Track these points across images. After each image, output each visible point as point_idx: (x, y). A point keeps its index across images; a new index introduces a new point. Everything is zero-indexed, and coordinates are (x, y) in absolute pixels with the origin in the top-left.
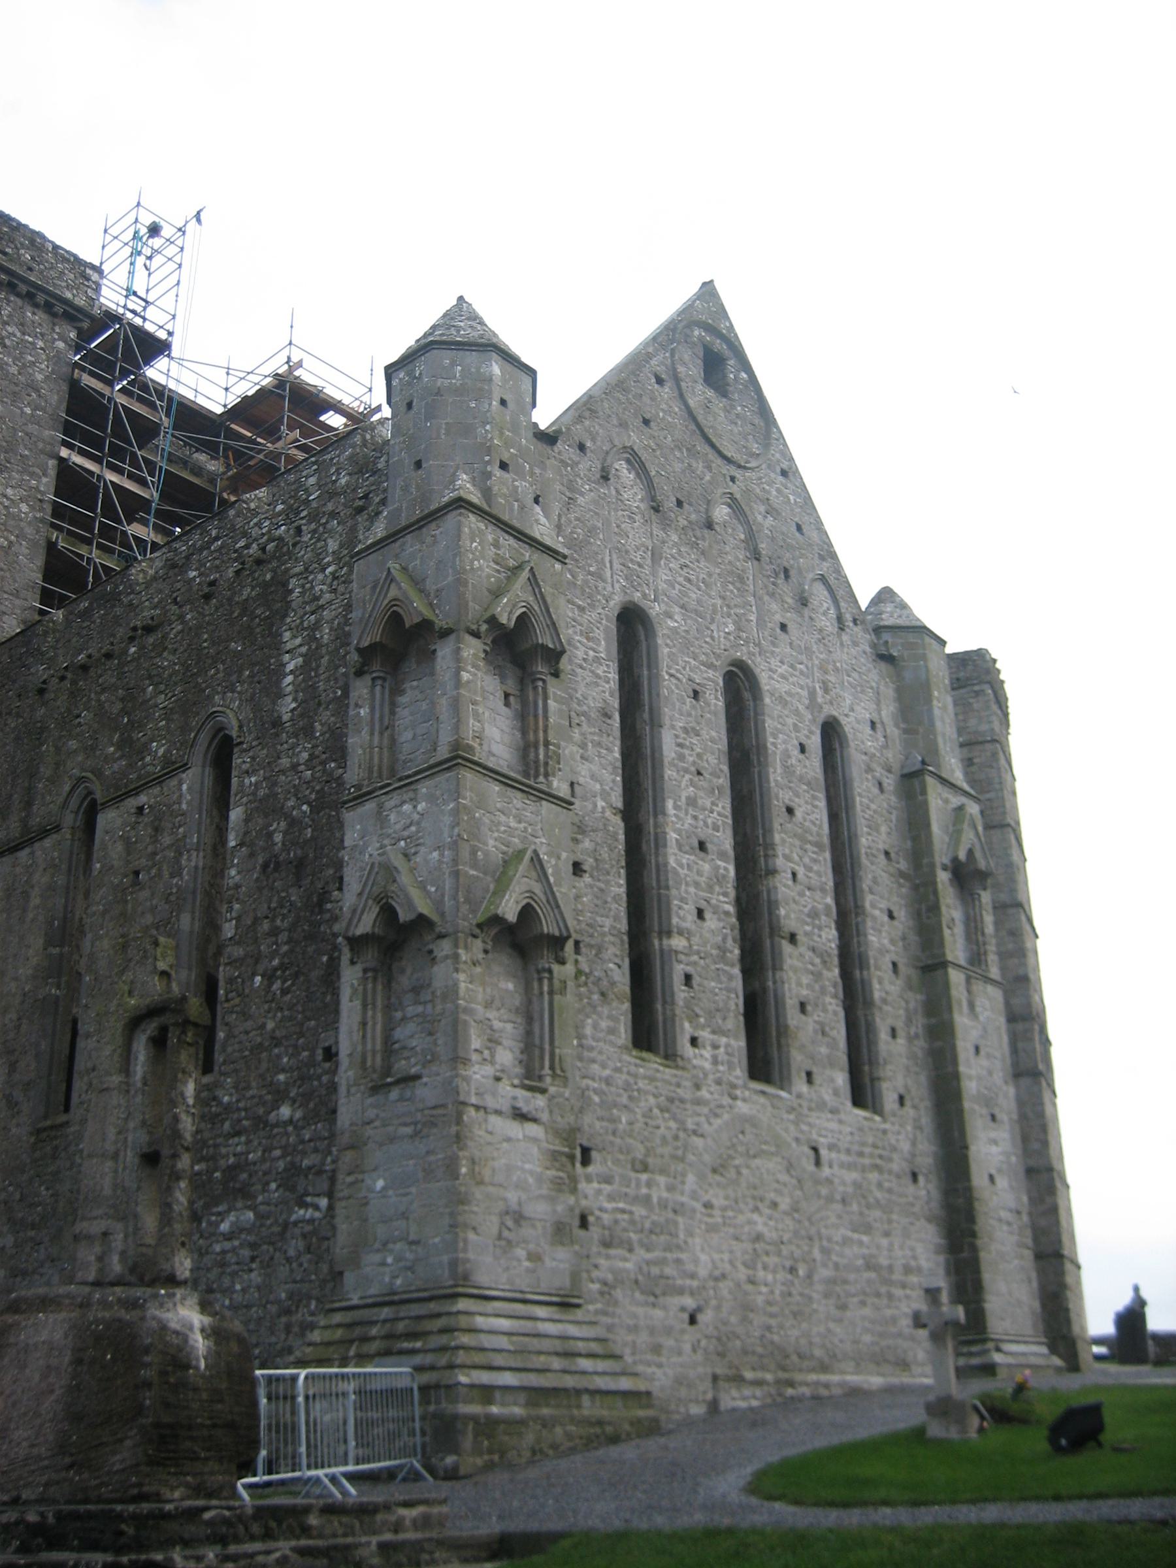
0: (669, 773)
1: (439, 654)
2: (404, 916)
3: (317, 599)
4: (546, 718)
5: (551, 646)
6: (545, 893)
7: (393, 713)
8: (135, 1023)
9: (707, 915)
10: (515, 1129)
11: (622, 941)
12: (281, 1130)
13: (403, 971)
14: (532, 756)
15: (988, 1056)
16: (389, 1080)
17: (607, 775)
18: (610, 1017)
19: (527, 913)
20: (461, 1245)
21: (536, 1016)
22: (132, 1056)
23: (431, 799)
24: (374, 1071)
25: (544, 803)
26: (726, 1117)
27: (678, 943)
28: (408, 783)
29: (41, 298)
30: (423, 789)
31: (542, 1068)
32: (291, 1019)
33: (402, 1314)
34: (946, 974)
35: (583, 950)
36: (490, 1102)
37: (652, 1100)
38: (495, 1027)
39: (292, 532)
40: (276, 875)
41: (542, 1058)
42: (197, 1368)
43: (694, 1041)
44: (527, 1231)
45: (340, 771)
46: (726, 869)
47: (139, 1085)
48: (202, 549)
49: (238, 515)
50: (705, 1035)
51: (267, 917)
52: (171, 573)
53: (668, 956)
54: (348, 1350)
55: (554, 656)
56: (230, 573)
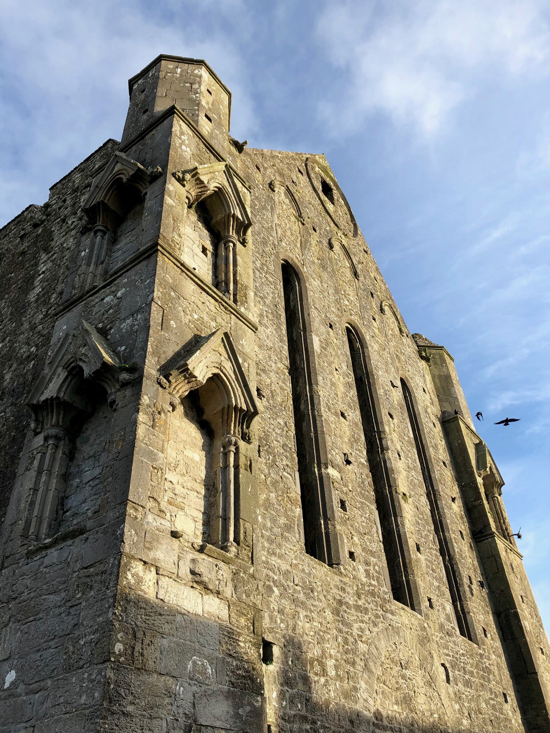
5: (240, 217)
11: (292, 458)
25: (232, 316)
38: (177, 492)
43: (351, 555)
46: (359, 435)
50: (358, 551)
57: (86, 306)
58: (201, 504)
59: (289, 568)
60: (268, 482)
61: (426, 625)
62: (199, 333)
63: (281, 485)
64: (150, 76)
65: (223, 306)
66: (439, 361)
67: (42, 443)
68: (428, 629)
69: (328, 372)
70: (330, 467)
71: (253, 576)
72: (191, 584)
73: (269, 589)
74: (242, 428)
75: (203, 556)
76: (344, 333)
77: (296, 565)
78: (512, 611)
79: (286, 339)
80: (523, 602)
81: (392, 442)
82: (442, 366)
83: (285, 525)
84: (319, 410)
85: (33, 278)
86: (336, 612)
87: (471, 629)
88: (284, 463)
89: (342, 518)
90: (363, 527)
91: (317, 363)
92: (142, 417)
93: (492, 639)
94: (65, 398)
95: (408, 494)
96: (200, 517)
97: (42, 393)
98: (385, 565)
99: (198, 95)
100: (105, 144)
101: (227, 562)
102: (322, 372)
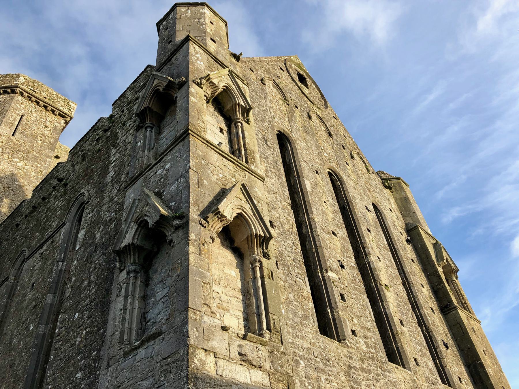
5: (243, 104)
25: (246, 172)
29: (49, 108)
38: (222, 299)
43: (353, 332)
46: (347, 246)
50: (358, 329)
57: (145, 179)
58: (240, 306)
59: (309, 346)
60: (287, 286)
61: (415, 378)
62: (224, 187)
63: (296, 288)
64: (170, 18)
65: (239, 166)
66: (398, 188)
67: (126, 276)
68: (417, 381)
69: (319, 204)
70: (329, 271)
71: (283, 353)
72: (240, 362)
73: (297, 362)
74: (263, 249)
75: (246, 342)
76: (327, 176)
77: (314, 343)
78: (478, 362)
79: (286, 184)
80: (485, 355)
81: (372, 249)
82: (401, 191)
83: (303, 315)
84: (317, 232)
85: (108, 166)
86: (348, 374)
87: (449, 379)
88: (296, 272)
89: (343, 306)
90: (359, 311)
91: (310, 199)
92: (192, 249)
93: (466, 384)
94: (138, 243)
95: (389, 285)
96: (241, 315)
97: (122, 242)
98: (379, 337)
99: (204, 26)
100: (146, 69)
101: (264, 344)
102: (315, 205)
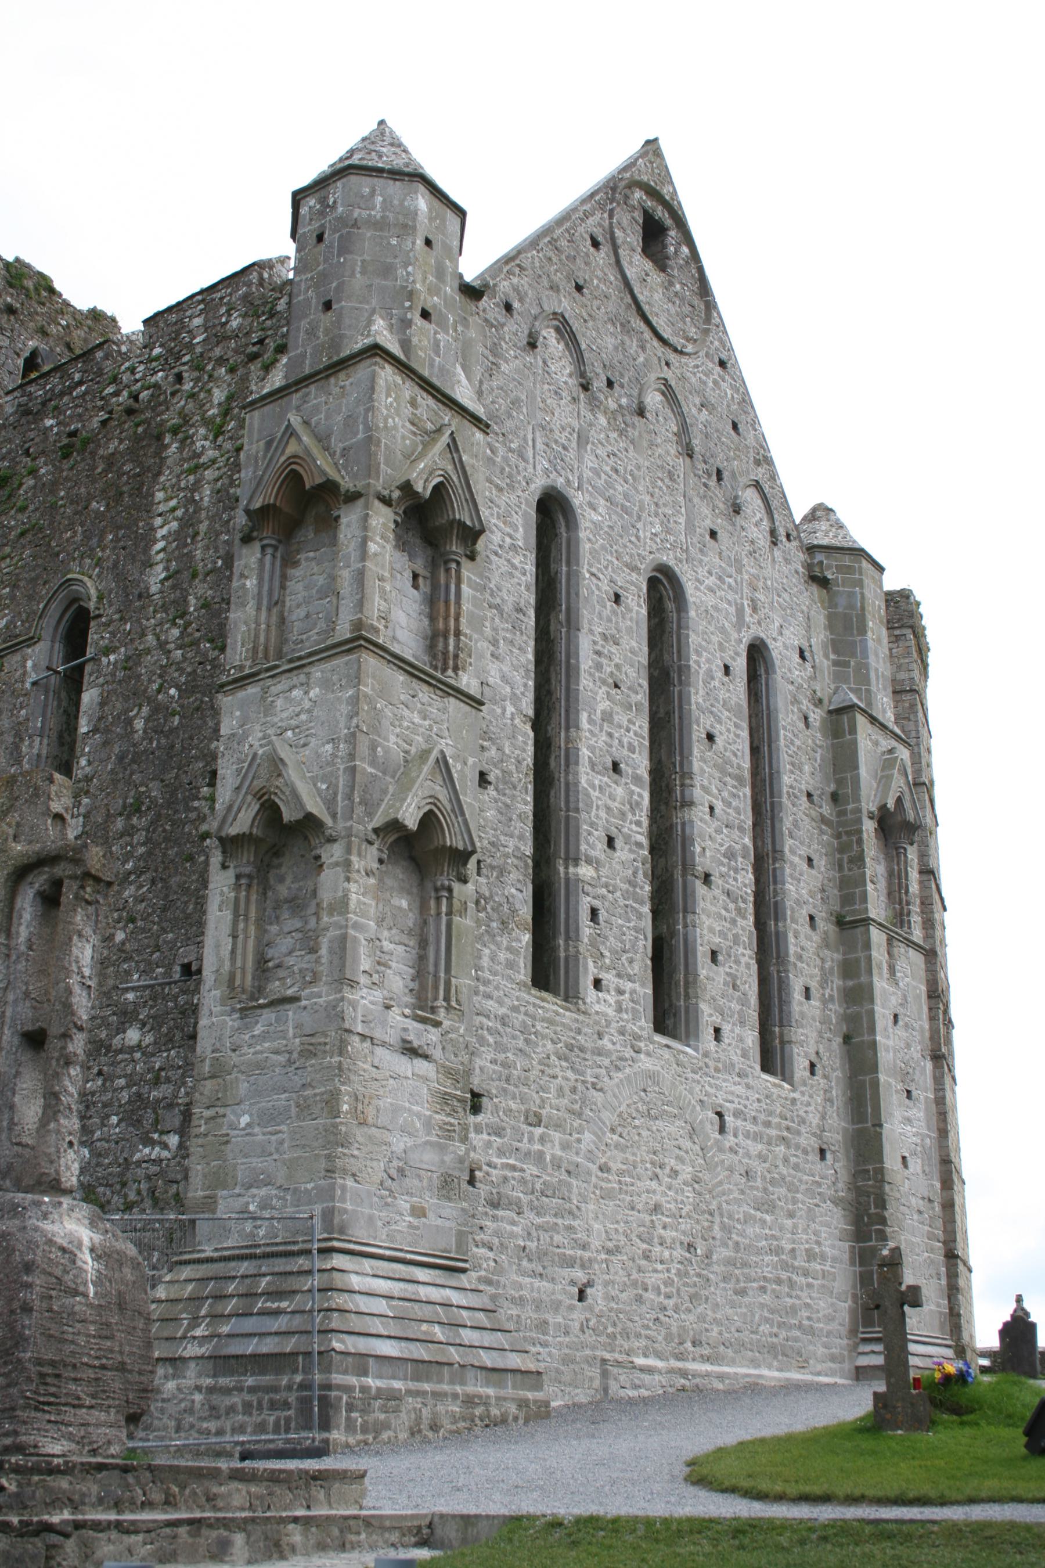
0: (586, 682)
1: (344, 521)
2: (288, 815)
3: (199, 456)
4: (458, 603)
5: (469, 523)
6: (450, 801)
7: (283, 587)
8: (22, 873)
9: (619, 843)
10: (405, 1065)
11: (526, 865)
12: (127, 1056)
13: (281, 880)
14: (440, 646)
15: (907, 1026)
16: (261, 1001)
17: (518, 678)
18: (509, 949)
19: (429, 820)
20: (339, 1192)
21: (432, 939)
22: (15, 914)
23: (326, 684)
24: (243, 991)
25: (452, 700)
26: (627, 1070)
27: (585, 871)
28: (299, 665)
30: (317, 672)
31: (436, 999)
32: (143, 930)
33: (264, 1269)
34: (868, 930)
35: (484, 871)
36: (378, 1034)
37: (550, 1046)
38: (385, 949)
39: (171, 379)
40: (135, 767)
41: (436, 988)
42: (85, 1295)
43: (597, 984)
44: (412, 1182)
45: (216, 653)
46: (640, 795)
47: (23, 948)
48: (62, 394)
49: (106, 357)
50: (609, 978)
51: (121, 815)
52: (23, 421)
53: (572, 885)
54: (199, 1308)
55: (471, 535)
56: (95, 423)
